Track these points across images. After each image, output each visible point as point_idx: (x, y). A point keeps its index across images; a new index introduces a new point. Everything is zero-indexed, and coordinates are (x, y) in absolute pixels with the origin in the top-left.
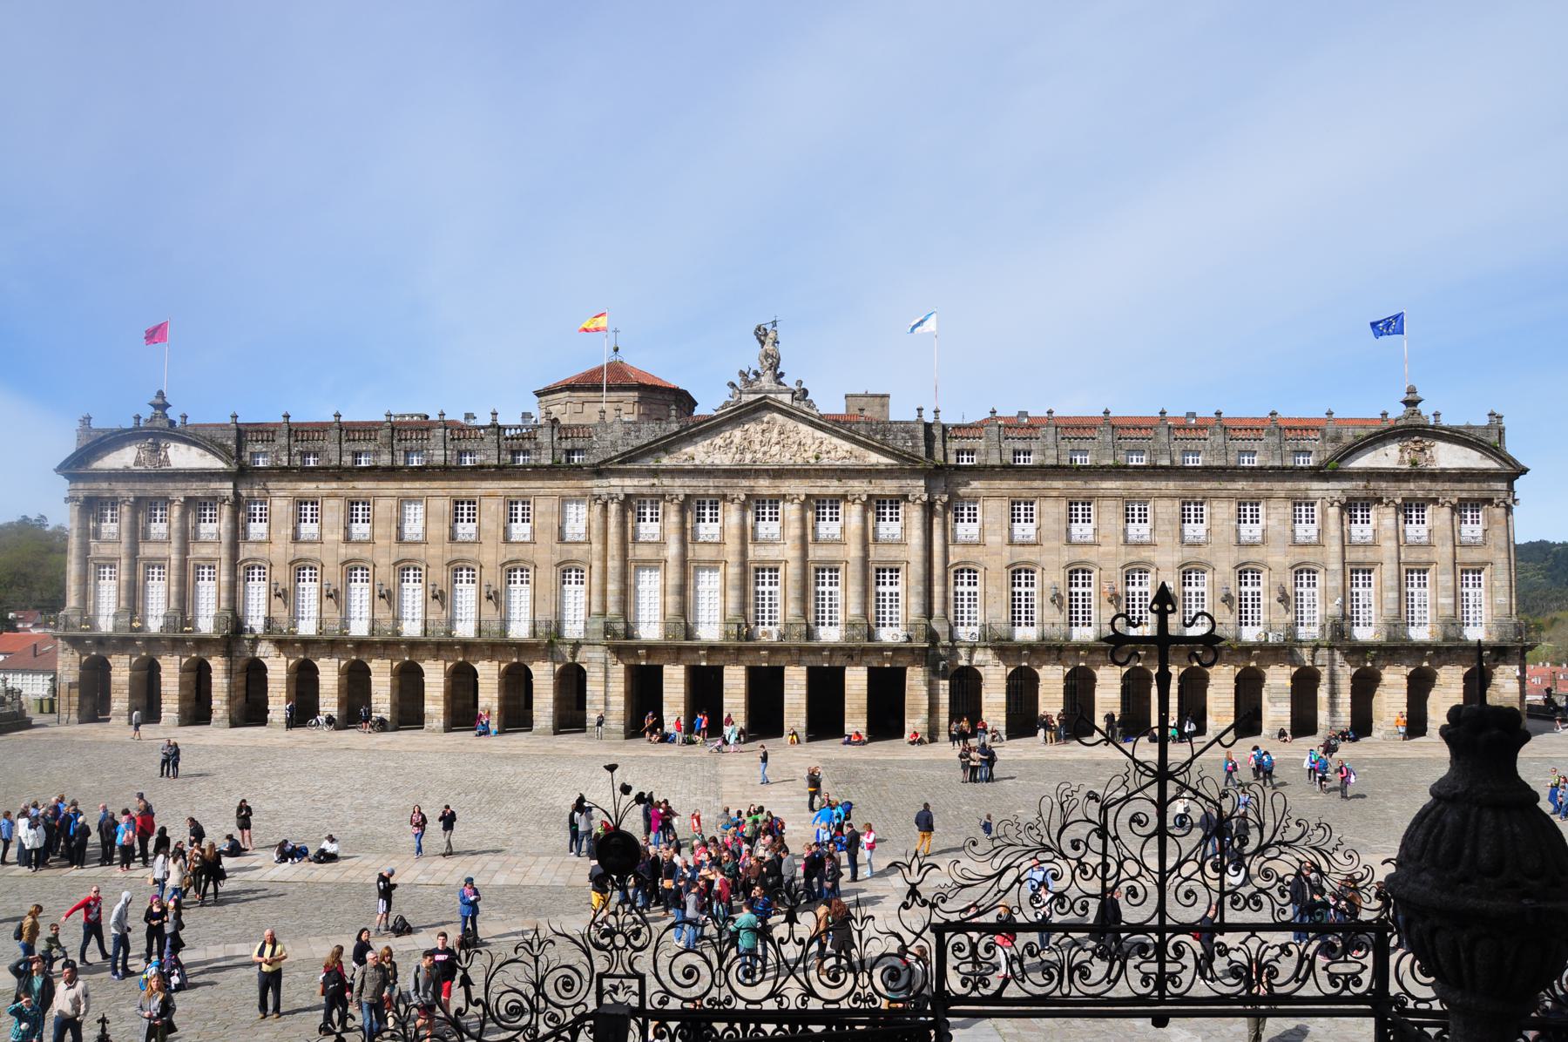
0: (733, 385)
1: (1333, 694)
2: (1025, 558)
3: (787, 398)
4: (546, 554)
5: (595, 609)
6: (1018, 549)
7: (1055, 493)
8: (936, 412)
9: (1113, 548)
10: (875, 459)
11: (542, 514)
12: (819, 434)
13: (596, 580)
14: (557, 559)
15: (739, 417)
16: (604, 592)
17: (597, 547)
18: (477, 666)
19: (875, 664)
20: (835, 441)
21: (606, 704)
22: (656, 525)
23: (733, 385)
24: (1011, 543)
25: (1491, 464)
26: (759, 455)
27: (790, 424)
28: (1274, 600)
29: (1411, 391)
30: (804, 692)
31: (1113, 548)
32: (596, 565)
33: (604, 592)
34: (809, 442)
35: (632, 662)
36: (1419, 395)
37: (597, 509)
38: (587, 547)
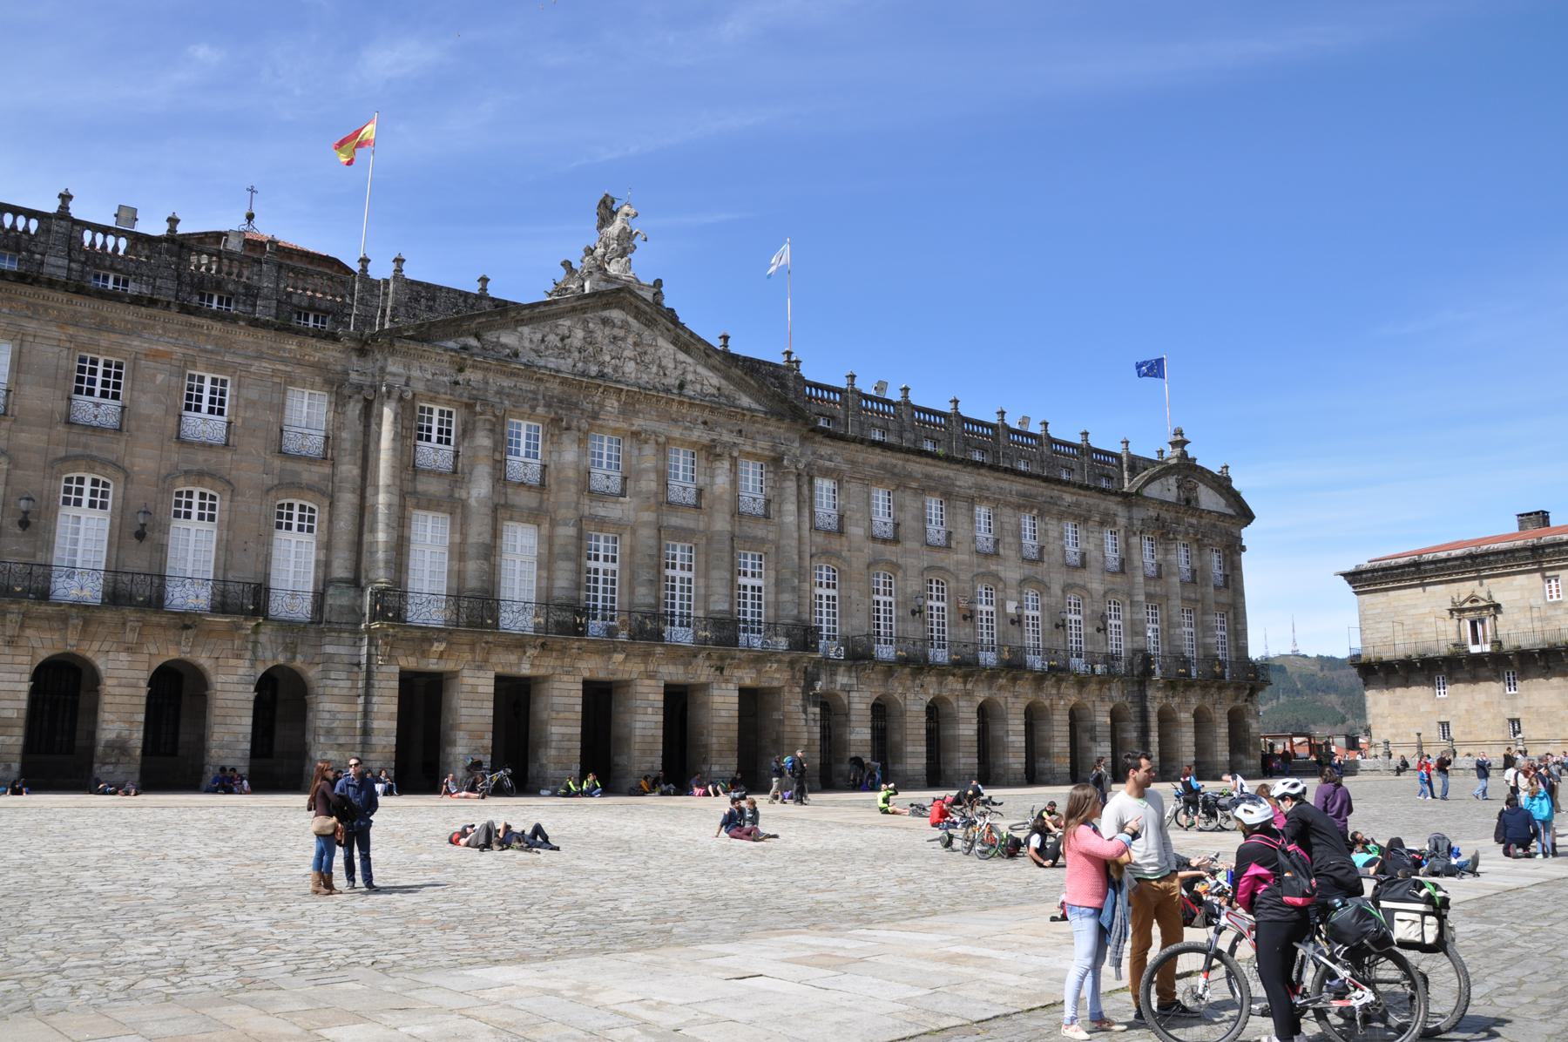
0: (567, 265)
1: (1144, 732)
2: (887, 556)
3: (649, 296)
4: (250, 468)
5: (340, 570)
6: (880, 547)
7: (914, 485)
8: (798, 362)
9: (965, 557)
10: (745, 401)
11: (251, 404)
12: (682, 356)
13: (345, 523)
14: (269, 480)
15: (584, 310)
16: (358, 546)
17: (349, 469)
18: (101, 663)
19: (748, 682)
20: (700, 369)
21: (366, 731)
22: (448, 450)
23: (567, 265)
24: (874, 538)
25: (1230, 511)
26: (608, 370)
27: (647, 333)
28: (1091, 630)
29: (1179, 432)
30: (661, 718)
31: (965, 557)
32: (347, 500)
33: (358, 546)
34: (671, 365)
35: (411, 663)
36: (1186, 437)
37: (354, 409)
38: (327, 470)
